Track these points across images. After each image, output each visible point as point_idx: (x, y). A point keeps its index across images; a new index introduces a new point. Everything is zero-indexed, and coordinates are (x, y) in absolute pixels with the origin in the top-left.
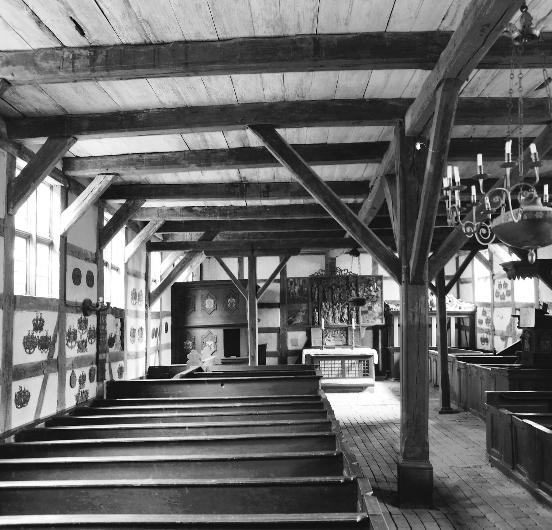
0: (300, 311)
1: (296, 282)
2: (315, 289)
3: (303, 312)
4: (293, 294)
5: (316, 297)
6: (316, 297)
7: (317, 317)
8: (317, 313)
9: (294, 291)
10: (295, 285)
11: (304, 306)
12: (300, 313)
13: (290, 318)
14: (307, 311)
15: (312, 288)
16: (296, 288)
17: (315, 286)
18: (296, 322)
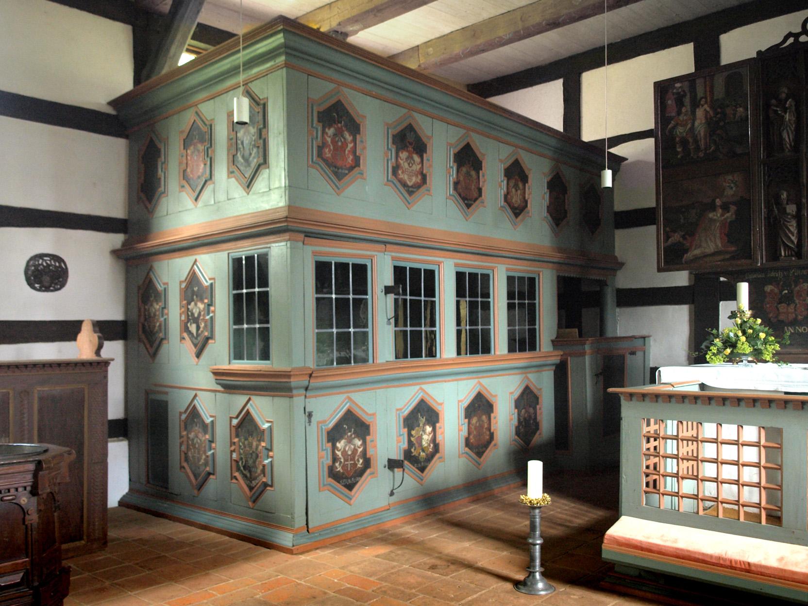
0: (712, 207)
1: (700, 93)
2: (782, 103)
3: (725, 207)
4: (684, 142)
5: (788, 137)
6: (788, 137)
7: (793, 226)
8: (791, 209)
9: (692, 128)
10: (695, 104)
11: (731, 186)
12: (716, 215)
13: (676, 237)
14: (744, 206)
15: (767, 106)
16: (700, 113)
17: (784, 92)
18: (697, 252)
